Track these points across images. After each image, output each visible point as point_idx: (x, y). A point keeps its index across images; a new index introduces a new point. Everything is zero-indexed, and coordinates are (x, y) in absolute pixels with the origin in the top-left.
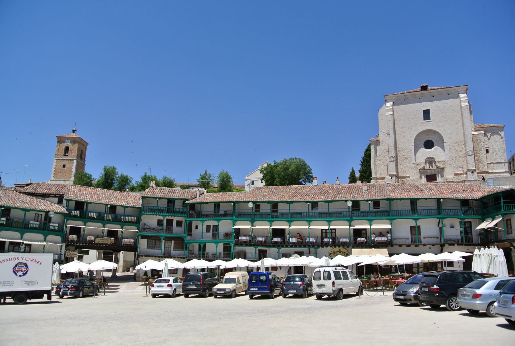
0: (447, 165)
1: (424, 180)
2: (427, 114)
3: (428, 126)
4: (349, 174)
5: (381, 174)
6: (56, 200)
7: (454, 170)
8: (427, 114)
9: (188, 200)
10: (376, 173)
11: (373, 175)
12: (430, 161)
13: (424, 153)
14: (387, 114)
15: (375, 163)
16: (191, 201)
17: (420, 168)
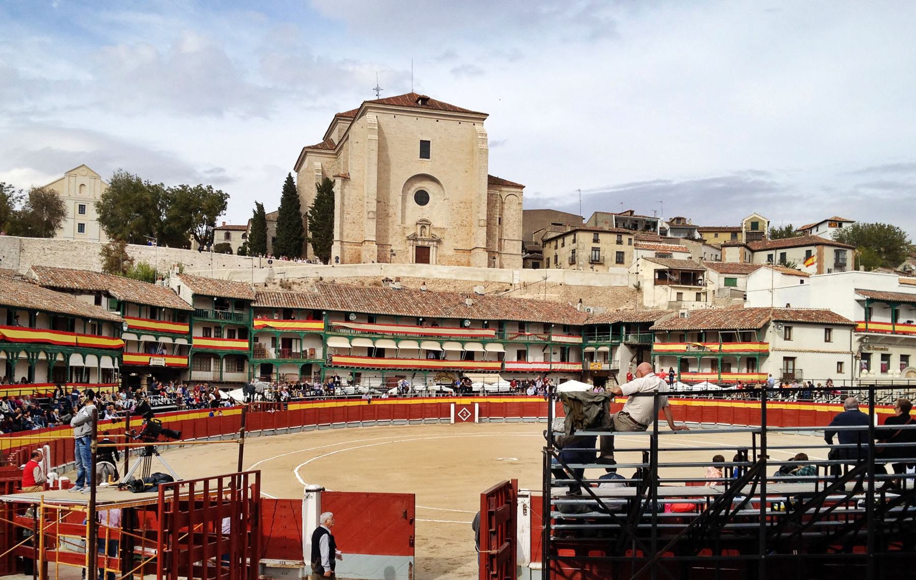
0: (446, 235)
1: (412, 252)
2: (425, 149)
3: (425, 167)
4: (252, 216)
5: (347, 236)
6: (93, 297)
7: (455, 245)
8: (425, 149)
9: (251, 301)
10: (341, 234)
11: (336, 236)
12: (424, 224)
13: (415, 212)
14: (369, 137)
15: (342, 217)
16: (256, 305)
17: (409, 233)
